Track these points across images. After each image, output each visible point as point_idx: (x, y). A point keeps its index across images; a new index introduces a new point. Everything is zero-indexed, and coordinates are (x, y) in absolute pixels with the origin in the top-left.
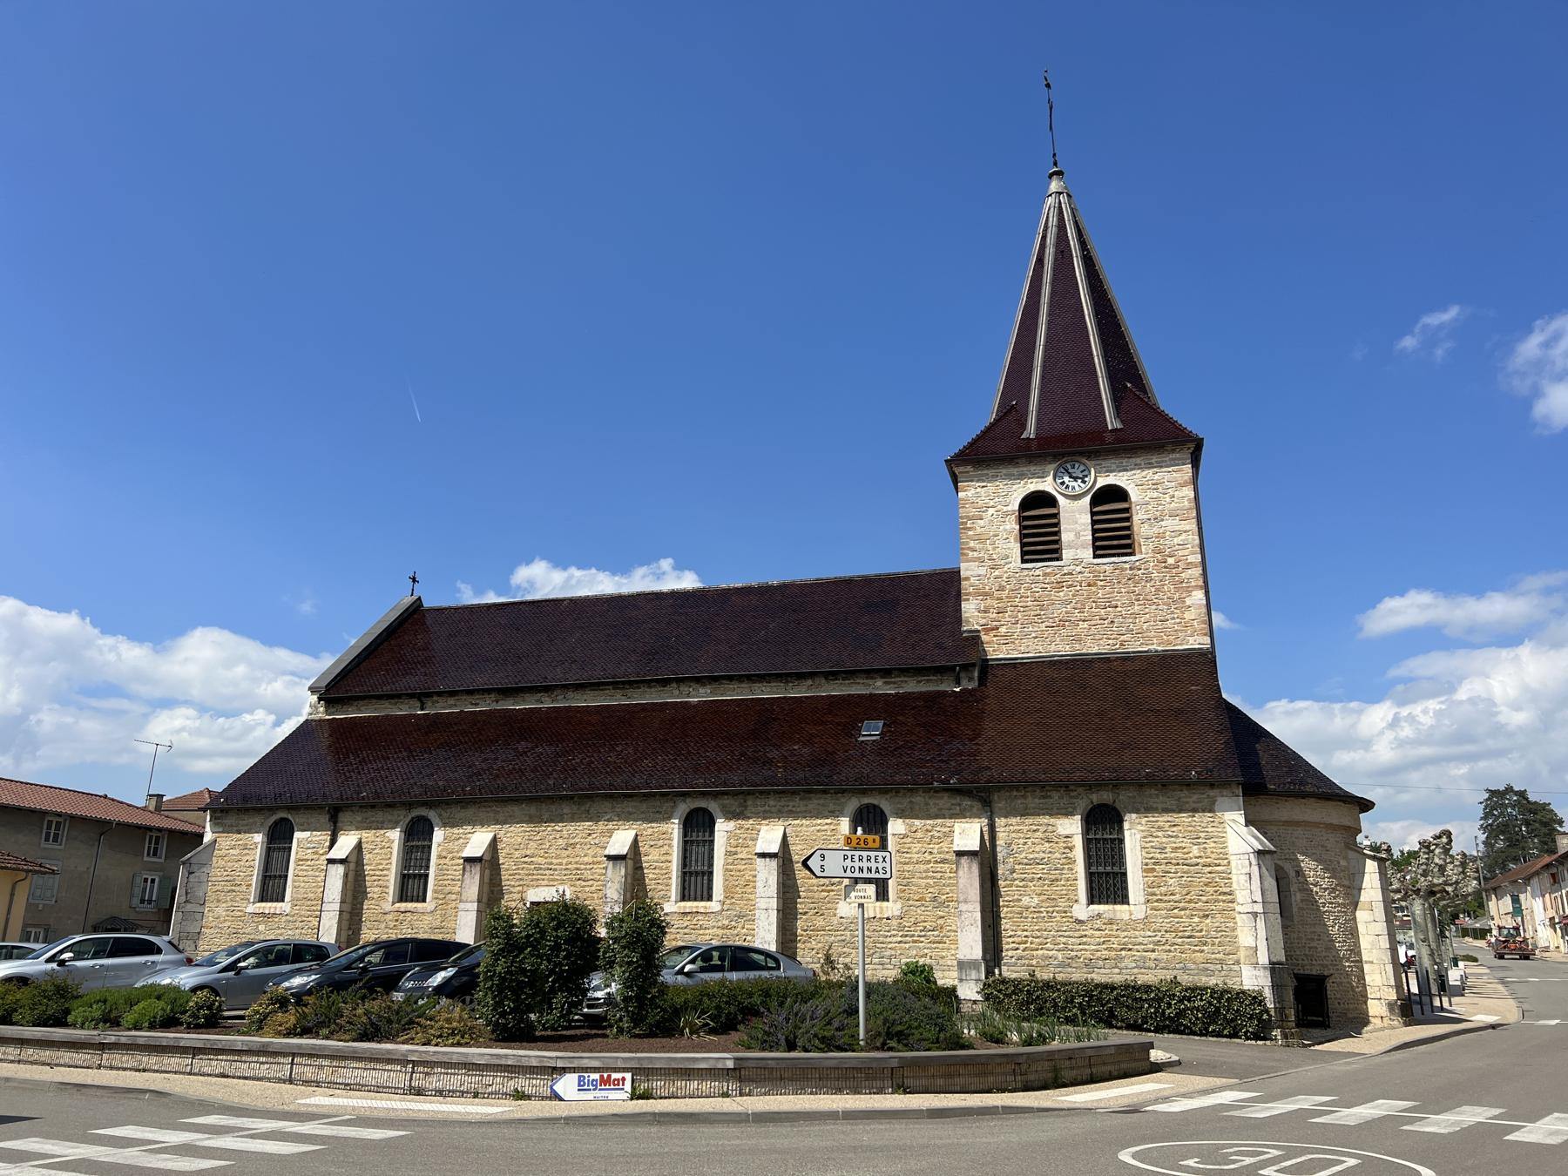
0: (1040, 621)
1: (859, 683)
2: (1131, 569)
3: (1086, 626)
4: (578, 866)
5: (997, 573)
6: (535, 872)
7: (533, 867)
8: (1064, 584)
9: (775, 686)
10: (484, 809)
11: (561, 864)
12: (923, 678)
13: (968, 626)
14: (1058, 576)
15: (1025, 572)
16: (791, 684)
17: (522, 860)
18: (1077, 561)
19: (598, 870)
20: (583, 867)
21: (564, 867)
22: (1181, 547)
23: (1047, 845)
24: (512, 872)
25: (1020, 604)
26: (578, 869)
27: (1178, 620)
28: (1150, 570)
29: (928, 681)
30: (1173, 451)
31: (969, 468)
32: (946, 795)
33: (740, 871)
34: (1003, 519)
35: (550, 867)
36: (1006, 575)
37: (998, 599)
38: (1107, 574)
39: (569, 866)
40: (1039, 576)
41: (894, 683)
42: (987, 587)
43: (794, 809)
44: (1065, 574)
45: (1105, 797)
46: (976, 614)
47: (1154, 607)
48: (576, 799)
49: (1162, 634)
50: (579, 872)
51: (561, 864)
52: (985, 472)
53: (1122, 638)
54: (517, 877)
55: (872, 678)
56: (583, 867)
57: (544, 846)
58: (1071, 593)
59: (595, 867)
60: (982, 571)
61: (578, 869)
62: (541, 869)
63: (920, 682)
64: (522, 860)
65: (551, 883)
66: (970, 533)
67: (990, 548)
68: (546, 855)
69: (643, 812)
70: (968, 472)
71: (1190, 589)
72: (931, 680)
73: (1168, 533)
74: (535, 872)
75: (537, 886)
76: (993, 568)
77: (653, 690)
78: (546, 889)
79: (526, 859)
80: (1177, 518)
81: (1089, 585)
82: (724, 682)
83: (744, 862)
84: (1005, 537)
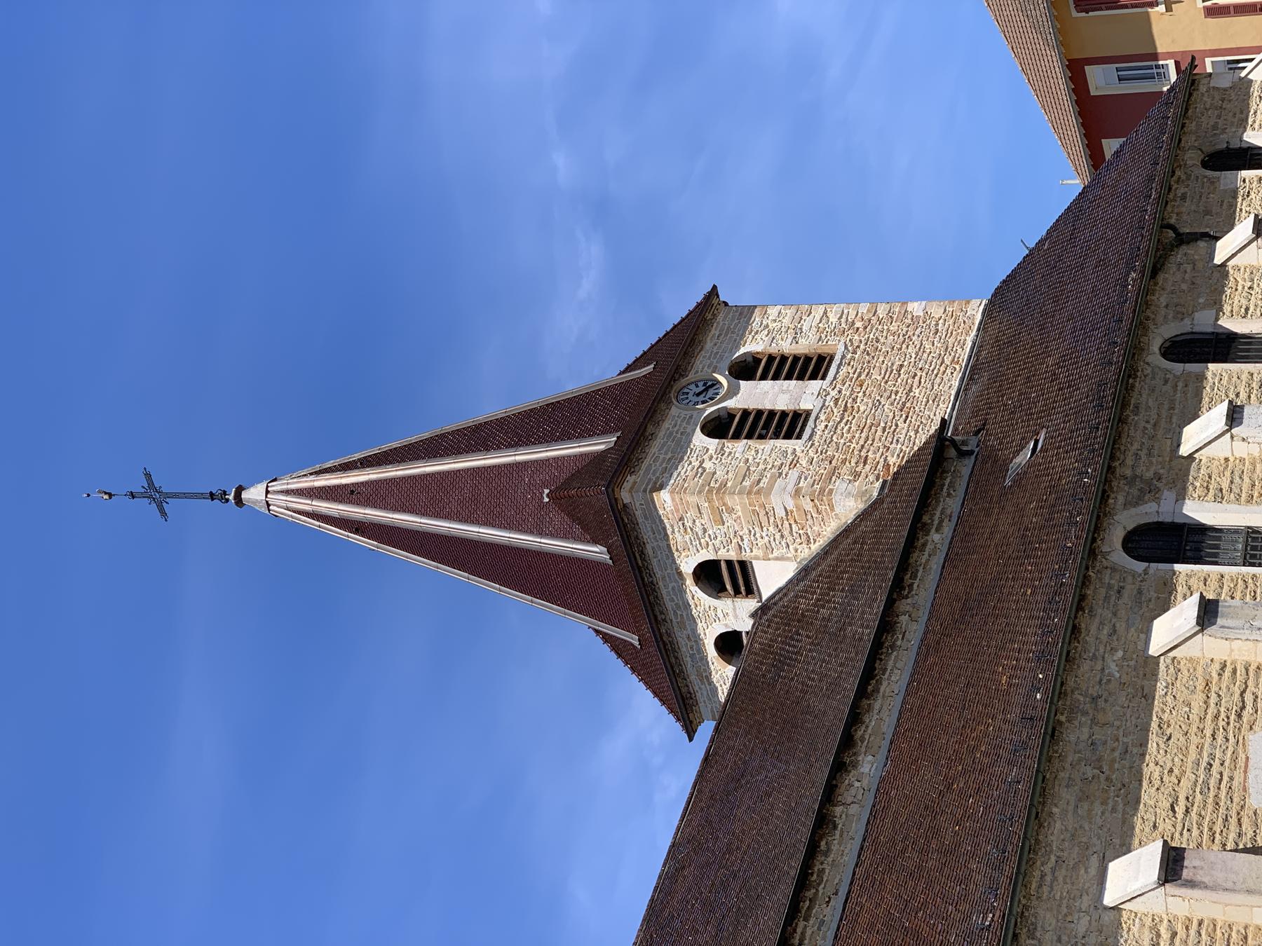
0: (894, 427)
1: (928, 561)
2: (854, 352)
3: (917, 391)
4: (1209, 717)
5: (804, 462)
6: (1212, 794)
7: (1199, 797)
8: (849, 405)
9: (895, 662)
10: (1045, 889)
11: (1200, 748)
12: (945, 490)
13: (873, 492)
14: (835, 410)
15: (816, 438)
16: (899, 643)
17: (1180, 815)
18: (823, 394)
19: (1224, 686)
20: (1212, 710)
21: (1209, 740)
22: (844, 317)
23: (1253, 195)
24: (1205, 837)
25: (861, 442)
26: (1216, 717)
27: (941, 321)
28: (863, 339)
29: (951, 485)
30: (714, 315)
31: (631, 479)
32: (1161, 277)
33: (1253, 485)
34: (726, 454)
35: (1204, 765)
36: (811, 454)
37: (844, 462)
38: (851, 371)
39: (1208, 732)
40: (826, 426)
41: (941, 522)
42: (822, 471)
43: (1152, 422)
44: (836, 404)
45: (1192, 158)
46: (857, 484)
47: (914, 338)
48: (1063, 718)
49: (954, 333)
50: (1223, 715)
51: (1200, 748)
52: (644, 466)
53: (947, 362)
54: (1217, 829)
55: (924, 545)
56: (1212, 710)
57: (1156, 775)
58: (865, 400)
59: (1214, 688)
60: (794, 474)
61: (1216, 717)
62: (1206, 783)
63: (949, 495)
64: (1180, 815)
65: (1241, 763)
66: (729, 484)
67: (762, 467)
68: (1176, 771)
69: (1115, 614)
70: (635, 483)
71: (903, 312)
72: (950, 482)
73: (820, 325)
74: (1212, 794)
75: (1245, 790)
76: (793, 464)
77: (835, 848)
78: (1251, 775)
79: (1180, 810)
80: (804, 318)
81: (861, 386)
82: (860, 733)
83: (1237, 480)
84: (753, 452)
